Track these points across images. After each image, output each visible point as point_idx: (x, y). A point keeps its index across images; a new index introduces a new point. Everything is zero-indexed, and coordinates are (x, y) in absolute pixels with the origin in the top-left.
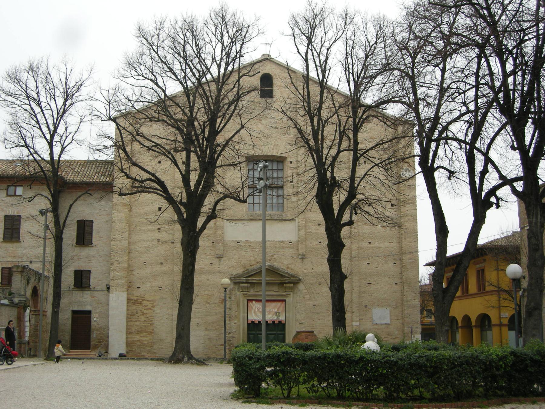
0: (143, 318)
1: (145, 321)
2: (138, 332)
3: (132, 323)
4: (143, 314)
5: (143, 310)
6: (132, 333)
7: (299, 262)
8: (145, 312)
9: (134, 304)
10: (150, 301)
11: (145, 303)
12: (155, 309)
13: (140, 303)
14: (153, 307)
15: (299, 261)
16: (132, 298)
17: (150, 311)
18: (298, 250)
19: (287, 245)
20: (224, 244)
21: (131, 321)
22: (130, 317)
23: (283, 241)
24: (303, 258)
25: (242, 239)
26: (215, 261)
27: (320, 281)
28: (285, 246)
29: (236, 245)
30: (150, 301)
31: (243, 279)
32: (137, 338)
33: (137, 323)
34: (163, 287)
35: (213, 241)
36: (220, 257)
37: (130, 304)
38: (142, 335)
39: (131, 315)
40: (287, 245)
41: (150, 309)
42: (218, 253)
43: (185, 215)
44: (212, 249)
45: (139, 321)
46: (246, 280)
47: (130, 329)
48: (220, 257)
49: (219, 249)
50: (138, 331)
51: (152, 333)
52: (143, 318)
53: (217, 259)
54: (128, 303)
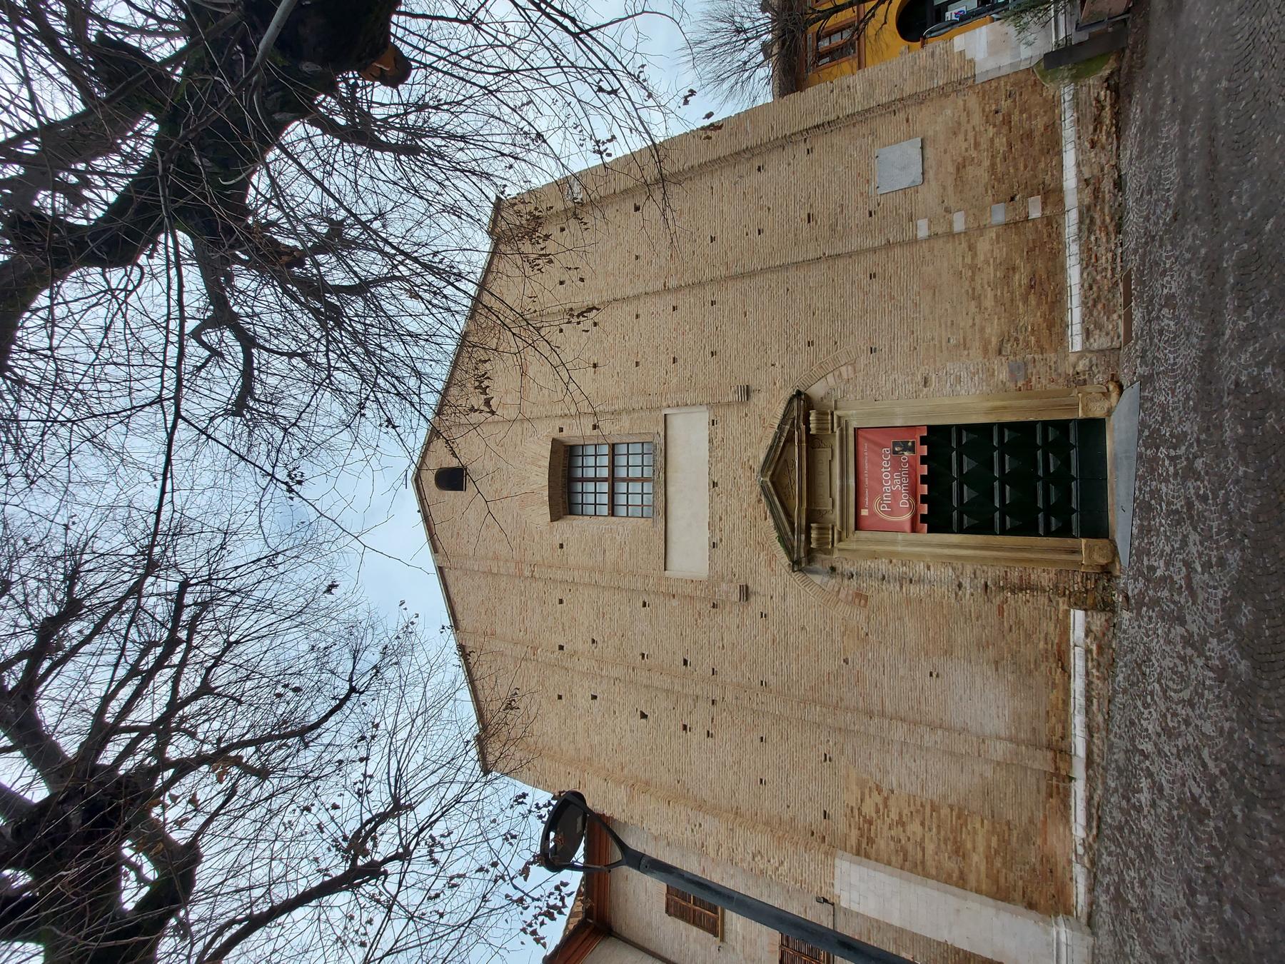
0: (914, 828)
1: (923, 824)
2: (959, 851)
3: (930, 863)
4: (901, 823)
5: (888, 821)
6: (961, 872)
7: (758, 400)
8: (894, 816)
9: (871, 841)
10: (863, 794)
11: (868, 809)
12: (885, 787)
13: (870, 823)
14: (880, 791)
15: (754, 398)
16: (853, 841)
17: (892, 802)
18: (729, 404)
19: (719, 431)
20: (714, 580)
21: (923, 862)
22: (909, 863)
23: (711, 441)
24: (747, 392)
25: (704, 538)
26: (756, 604)
27: (803, 343)
28: (720, 436)
29: (718, 551)
30: (863, 794)
31: (798, 540)
32: (977, 859)
33: (930, 848)
34: (823, 749)
35: (709, 606)
36: (746, 593)
37: (873, 852)
38: (969, 846)
39: (905, 860)
40: (719, 431)
41: (886, 800)
42: (735, 597)
43: (552, 845)
44: (727, 609)
45: (923, 839)
46: (800, 533)
47: (950, 876)
48: (746, 593)
49: (727, 593)
50: (957, 852)
51: (962, 814)
52: (914, 828)
53: (752, 599)
54: (867, 856)
